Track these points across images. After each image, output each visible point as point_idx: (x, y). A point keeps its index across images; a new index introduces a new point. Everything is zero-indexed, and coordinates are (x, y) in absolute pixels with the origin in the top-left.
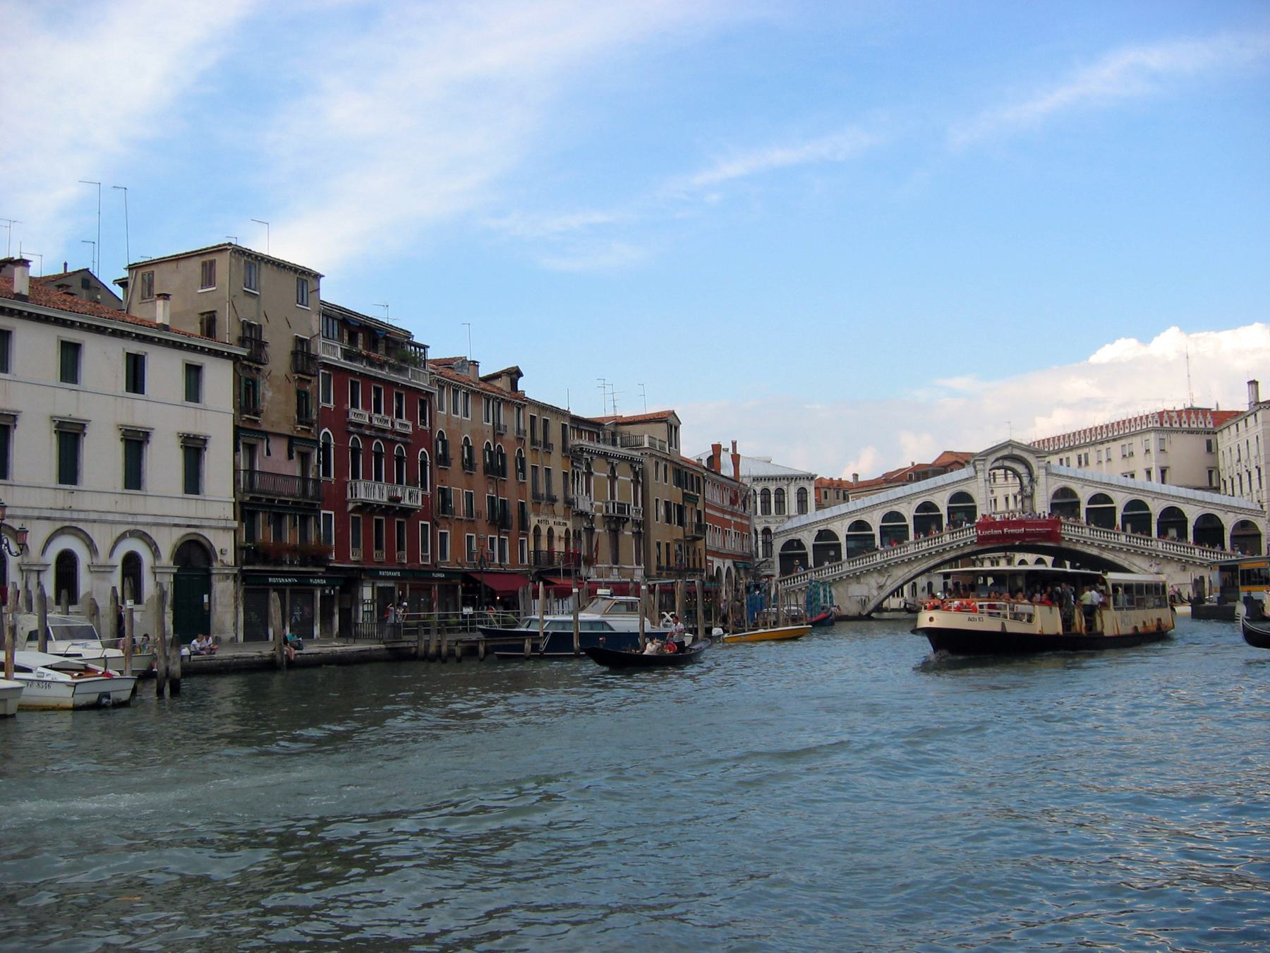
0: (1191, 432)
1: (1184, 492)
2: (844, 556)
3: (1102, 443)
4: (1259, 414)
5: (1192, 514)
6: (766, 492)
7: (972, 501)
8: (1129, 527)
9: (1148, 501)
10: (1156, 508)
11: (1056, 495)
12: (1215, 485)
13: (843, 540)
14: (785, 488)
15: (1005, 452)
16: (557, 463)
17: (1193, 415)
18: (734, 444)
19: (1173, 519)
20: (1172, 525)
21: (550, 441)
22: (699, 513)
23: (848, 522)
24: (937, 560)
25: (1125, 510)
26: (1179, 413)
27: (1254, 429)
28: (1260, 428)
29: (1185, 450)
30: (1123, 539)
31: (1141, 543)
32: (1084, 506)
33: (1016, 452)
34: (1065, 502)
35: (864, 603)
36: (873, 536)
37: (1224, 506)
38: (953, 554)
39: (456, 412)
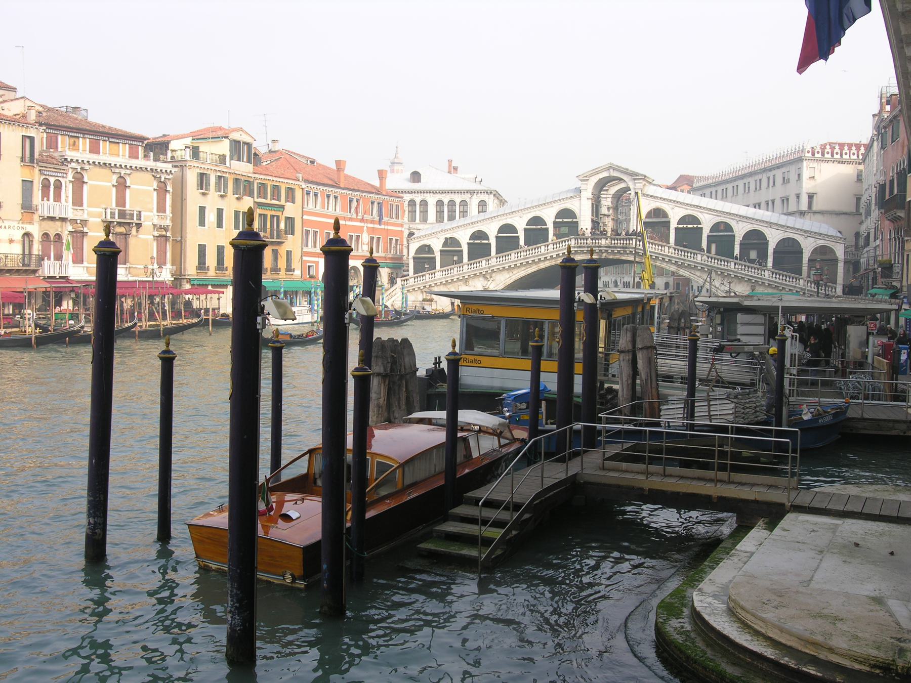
3: (770, 170)
5: (773, 238)
6: (452, 203)
8: (713, 247)
9: (733, 223)
11: (649, 215)
14: (468, 200)
15: (605, 174)
17: (846, 148)
18: (450, 161)
19: (755, 240)
23: (470, 231)
25: (711, 230)
32: (673, 225)
36: (490, 244)
37: (805, 231)
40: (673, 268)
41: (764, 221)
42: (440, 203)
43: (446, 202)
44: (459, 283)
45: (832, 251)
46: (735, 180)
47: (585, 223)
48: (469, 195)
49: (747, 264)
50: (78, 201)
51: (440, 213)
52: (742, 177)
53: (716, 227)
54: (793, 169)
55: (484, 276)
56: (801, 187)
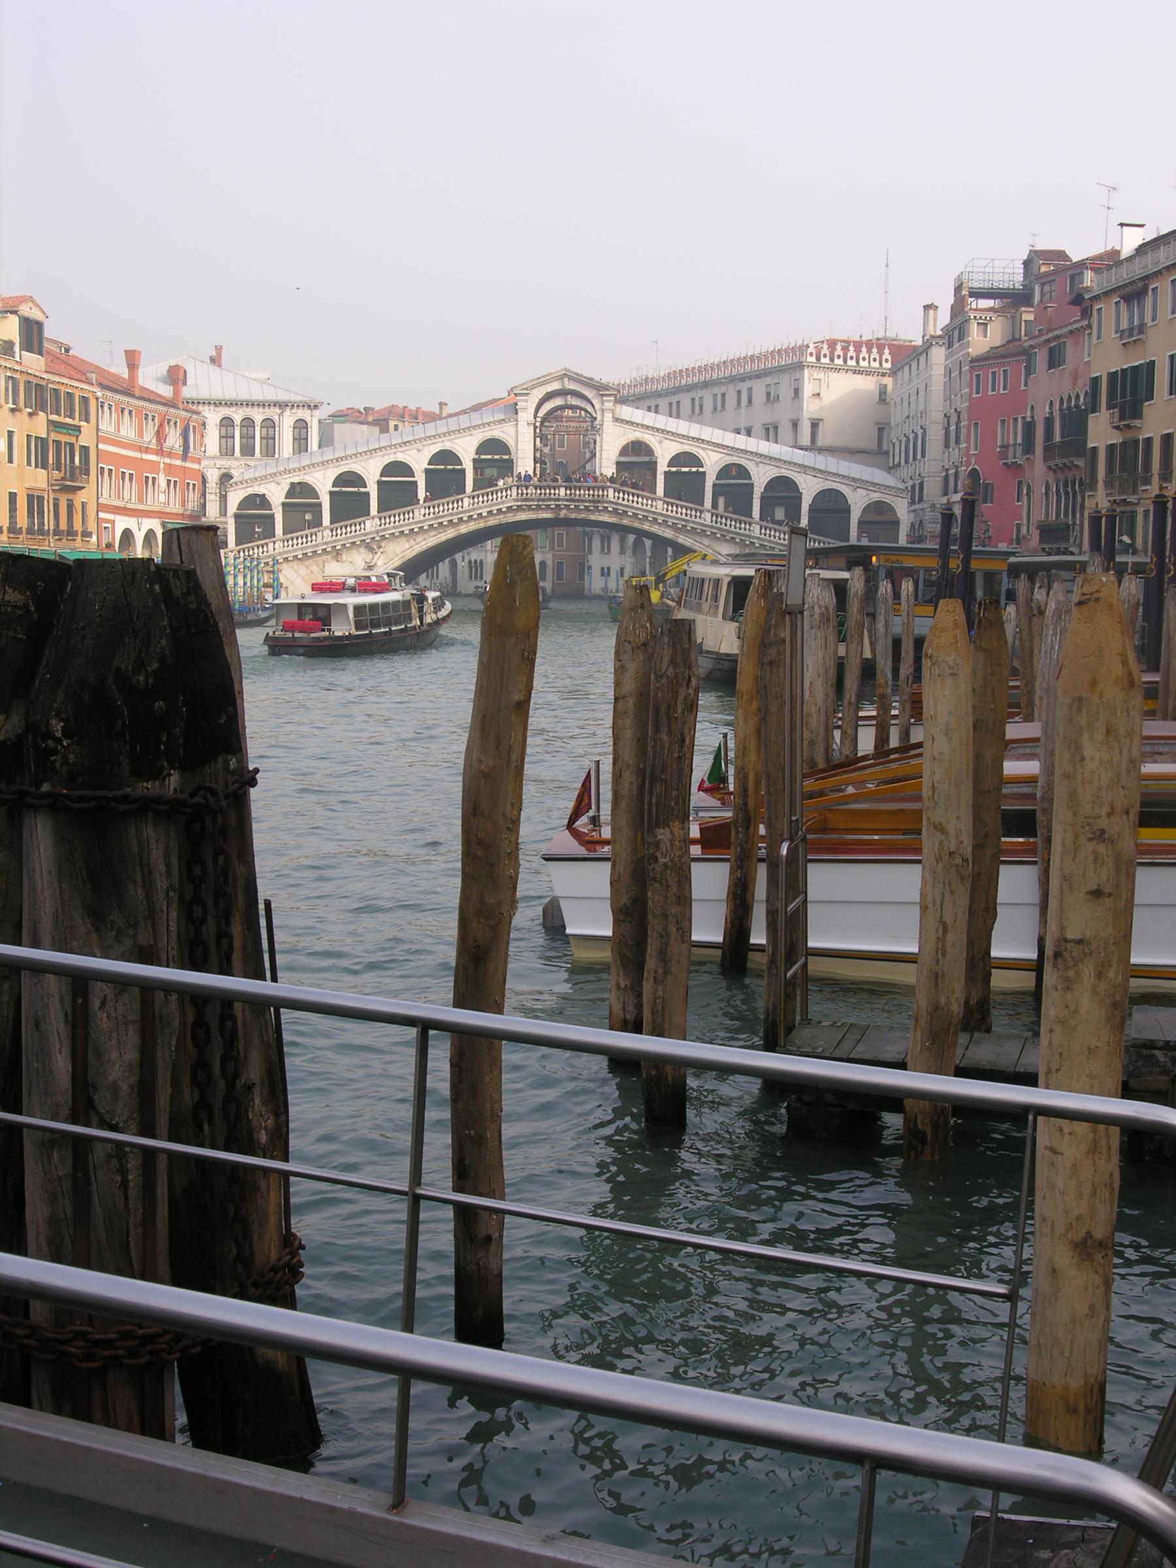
0: (858, 372)
1: (799, 456)
2: (326, 521)
3: (743, 380)
5: (809, 487)
6: (248, 423)
7: (510, 454)
8: (721, 501)
9: (750, 466)
10: (761, 476)
11: (624, 451)
12: (885, 448)
14: (276, 418)
15: (556, 386)
17: (864, 349)
18: (219, 349)
20: (779, 501)
22: (85, 450)
23: (332, 473)
24: (450, 534)
31: (731, 526)
32: (662, 467)
36: (368, 494)
37: (854, 480)
41: (795, 464)
42: (227, 422)
43: (238, 421)
44: (325, 558)
45: (891, 509)
46: (674, 393)
47: (525, 464)
48: (278, 410)
49: (770, 525)
51: (226, 437)
52: (689, 388)
53: (725, 472)
54: (785, 380)
56: (800, 409)
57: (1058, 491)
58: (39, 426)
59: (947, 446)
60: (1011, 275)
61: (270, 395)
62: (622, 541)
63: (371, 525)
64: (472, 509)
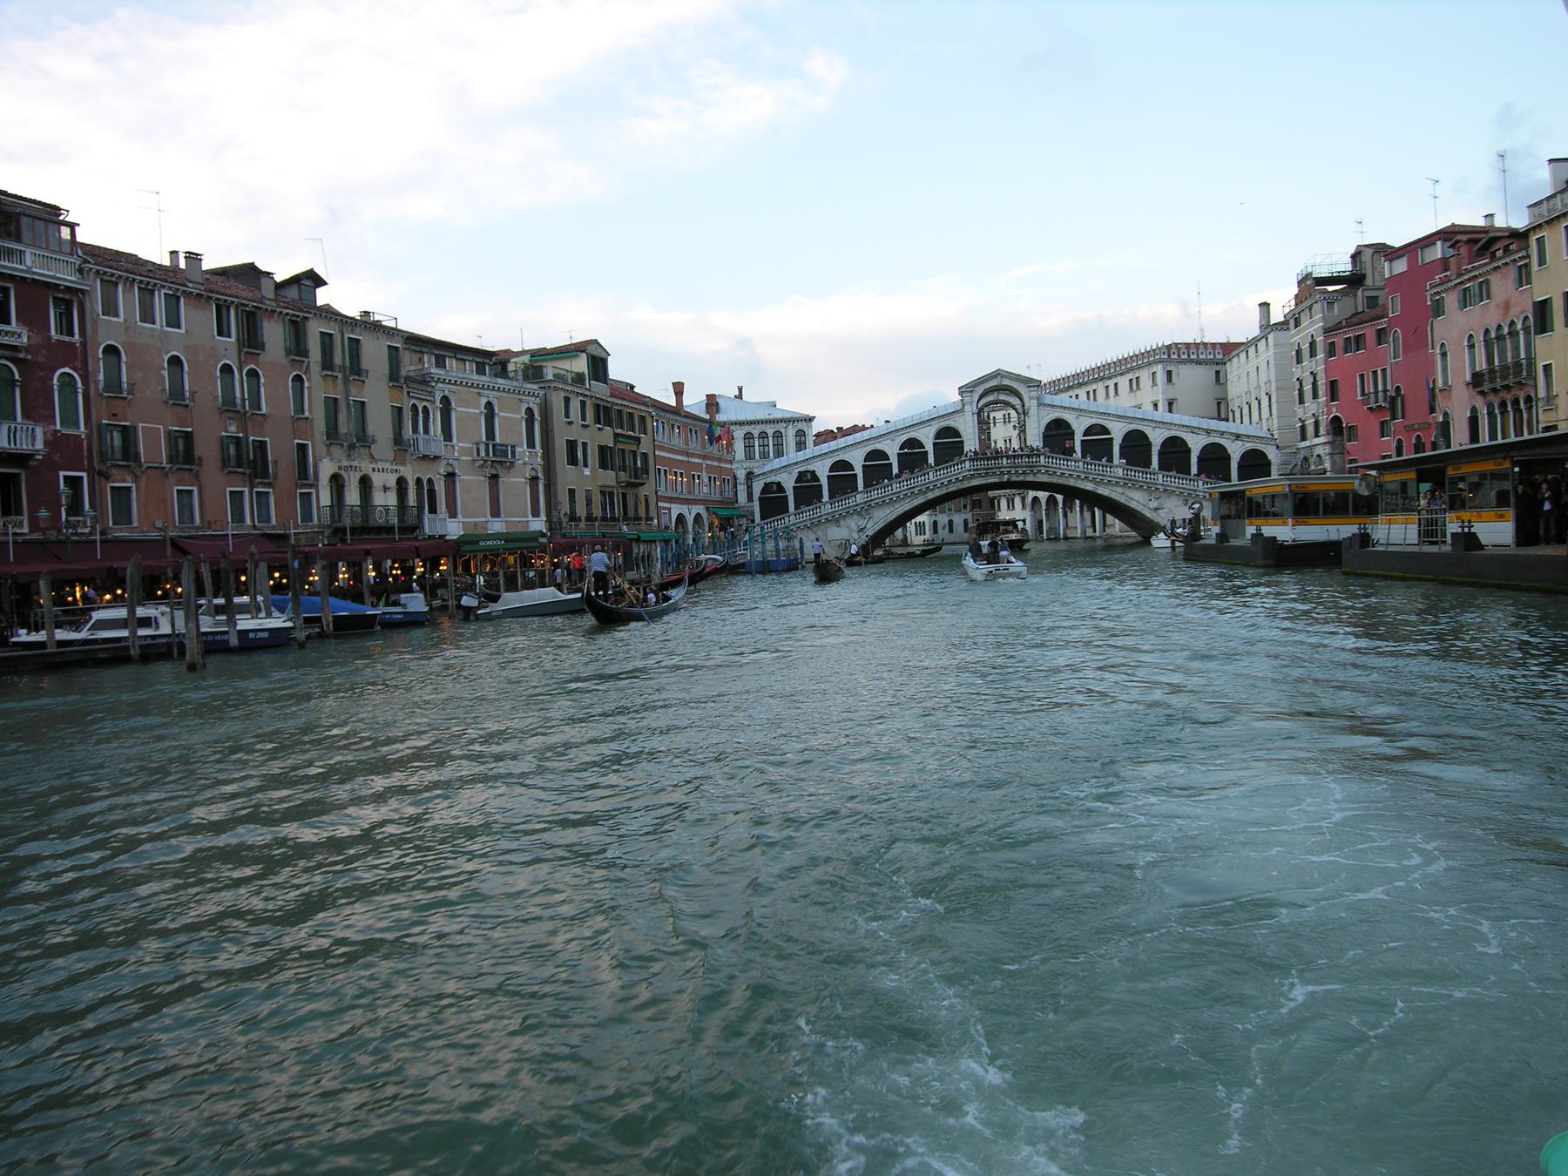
0: (1199, 362)
1: (1187, 420)
2: (826, 498)
4: (1271, 337)
5: (1196, 444)
6: (763, 435)
10: (1157, 438)
13: (824, 482)
15: (994, 383)
16: (377, 396)
21: (365, 365)
23: (829, 462)
26: (1188, 345)
27: (1266, 353)
28: (1271, 350)
29: (1193, 378)
30: (1120, 472)
32: (1078, 438)
33: (1006, 382)
34: (1058, 433)
35: (846, 544)
38: (937, 493)
39: (148, 316)
40: (1089, 486)
50: (448, 436)
51: (749, 447)
55: (859, 514)
57: (1491, 414)
58: (607, 437)
59: (1301, 401)
60: (1344, 266)
61: (778, 416)
62: (1023, 499)
63: (860, 498)
64: (937, 479)
